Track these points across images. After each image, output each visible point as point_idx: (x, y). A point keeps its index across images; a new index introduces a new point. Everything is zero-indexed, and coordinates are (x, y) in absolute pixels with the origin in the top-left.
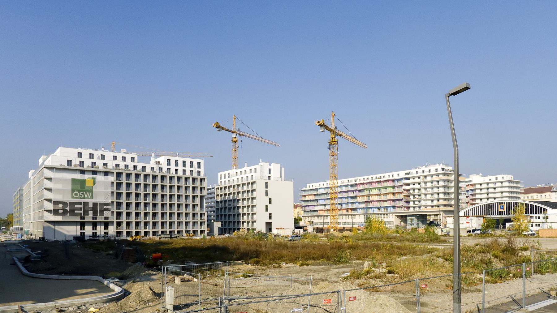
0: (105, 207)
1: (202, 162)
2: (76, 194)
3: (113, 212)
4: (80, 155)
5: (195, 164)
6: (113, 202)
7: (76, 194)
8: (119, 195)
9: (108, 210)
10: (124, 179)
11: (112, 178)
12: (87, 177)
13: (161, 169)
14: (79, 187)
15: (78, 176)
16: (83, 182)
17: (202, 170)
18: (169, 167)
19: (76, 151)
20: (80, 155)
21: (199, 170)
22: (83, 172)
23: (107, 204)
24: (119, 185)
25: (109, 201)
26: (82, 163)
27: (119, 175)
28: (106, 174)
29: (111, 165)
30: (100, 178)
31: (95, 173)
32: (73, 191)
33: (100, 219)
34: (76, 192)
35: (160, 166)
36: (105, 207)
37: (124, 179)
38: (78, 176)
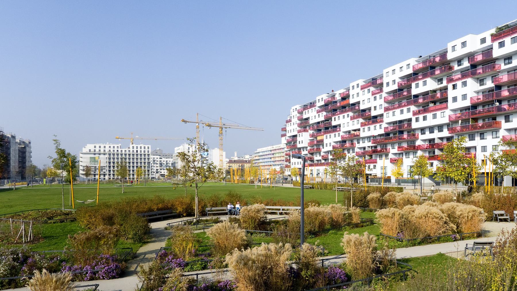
0: (103, 168)
1: (150, 146)
2: (92, 163)
3: (107, 170)
4: (95, 147)
5: (146, 148)
6: (107, 166)
7: (92, 163)
8: (110, 163)
9: (105, 169)
10: (112, 156)
11: (107, 156)
12: (97, 156)
13: (129, 151)
14: (93, 160)
15: (93, 156)
16: (95, 158)
17: (150, 150)
18: (133, 150)
19: (94, 145)
20: (95, 147)
21: (148, 150)
22: (95, 154)
23: (105, 167)
24: (110, 159)
25: (105, 165)
26: (95, 150)
27: (110, 154)
28: (104, 154)
29: (107, 150)
30: (102, 156)
31: (100, 154)
32: (90, 162)
33: (102, 173)
34: (92, 162)
35: (129, 149)
36: (103, 168)
37: (112, 156)
38: (93, 156)
